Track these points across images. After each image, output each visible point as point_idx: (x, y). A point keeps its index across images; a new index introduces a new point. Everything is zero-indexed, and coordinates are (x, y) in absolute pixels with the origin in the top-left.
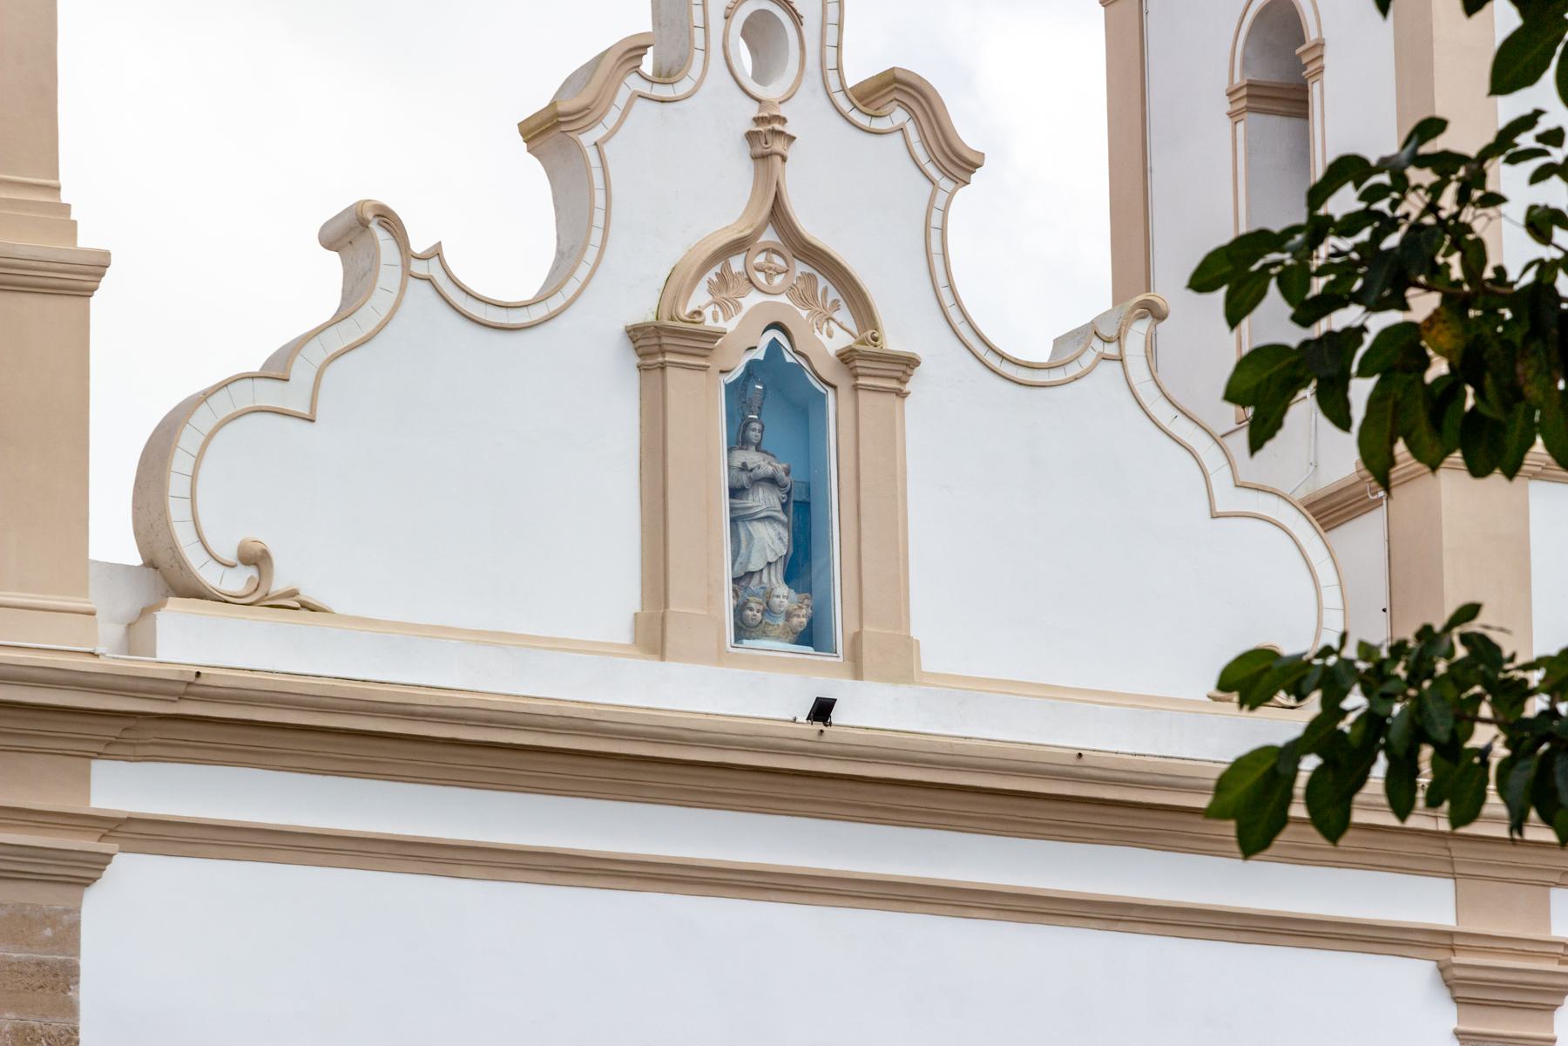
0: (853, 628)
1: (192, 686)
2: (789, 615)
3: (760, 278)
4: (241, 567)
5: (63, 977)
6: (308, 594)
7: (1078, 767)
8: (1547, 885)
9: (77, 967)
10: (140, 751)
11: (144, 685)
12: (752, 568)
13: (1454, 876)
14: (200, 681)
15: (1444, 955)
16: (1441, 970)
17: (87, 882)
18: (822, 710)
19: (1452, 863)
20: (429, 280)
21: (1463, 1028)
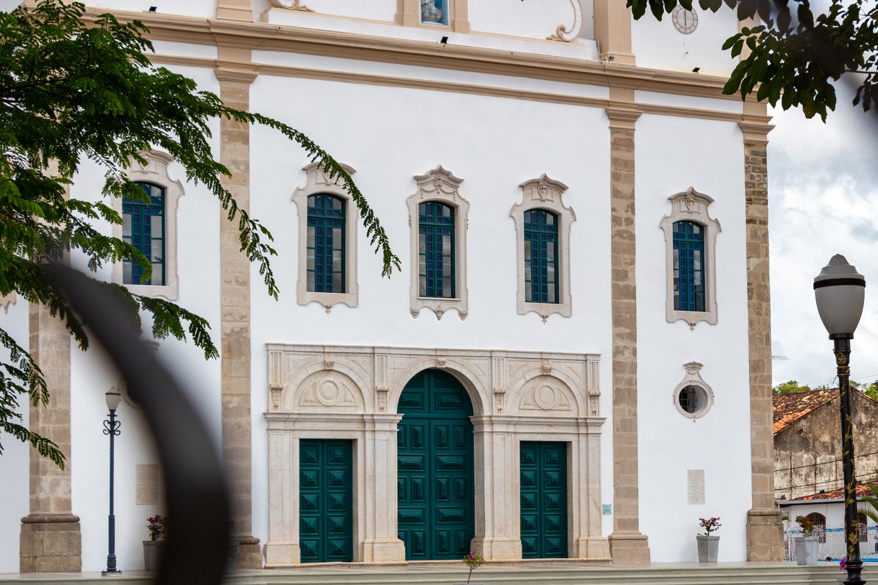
0: (453, 19)
1: (278, 31)
2: (436, 15)
6: (309, 7)
7: (511, 56)
8: (634, 89)
9: (248, 105)
10: (264, 48)
11: (266, 30)
13: (609, 86)
15: (607, 107)
16: (606, 111)
17: (251, 82)
18: (444, 40)
19: (609, 83)
21: (611, 126)
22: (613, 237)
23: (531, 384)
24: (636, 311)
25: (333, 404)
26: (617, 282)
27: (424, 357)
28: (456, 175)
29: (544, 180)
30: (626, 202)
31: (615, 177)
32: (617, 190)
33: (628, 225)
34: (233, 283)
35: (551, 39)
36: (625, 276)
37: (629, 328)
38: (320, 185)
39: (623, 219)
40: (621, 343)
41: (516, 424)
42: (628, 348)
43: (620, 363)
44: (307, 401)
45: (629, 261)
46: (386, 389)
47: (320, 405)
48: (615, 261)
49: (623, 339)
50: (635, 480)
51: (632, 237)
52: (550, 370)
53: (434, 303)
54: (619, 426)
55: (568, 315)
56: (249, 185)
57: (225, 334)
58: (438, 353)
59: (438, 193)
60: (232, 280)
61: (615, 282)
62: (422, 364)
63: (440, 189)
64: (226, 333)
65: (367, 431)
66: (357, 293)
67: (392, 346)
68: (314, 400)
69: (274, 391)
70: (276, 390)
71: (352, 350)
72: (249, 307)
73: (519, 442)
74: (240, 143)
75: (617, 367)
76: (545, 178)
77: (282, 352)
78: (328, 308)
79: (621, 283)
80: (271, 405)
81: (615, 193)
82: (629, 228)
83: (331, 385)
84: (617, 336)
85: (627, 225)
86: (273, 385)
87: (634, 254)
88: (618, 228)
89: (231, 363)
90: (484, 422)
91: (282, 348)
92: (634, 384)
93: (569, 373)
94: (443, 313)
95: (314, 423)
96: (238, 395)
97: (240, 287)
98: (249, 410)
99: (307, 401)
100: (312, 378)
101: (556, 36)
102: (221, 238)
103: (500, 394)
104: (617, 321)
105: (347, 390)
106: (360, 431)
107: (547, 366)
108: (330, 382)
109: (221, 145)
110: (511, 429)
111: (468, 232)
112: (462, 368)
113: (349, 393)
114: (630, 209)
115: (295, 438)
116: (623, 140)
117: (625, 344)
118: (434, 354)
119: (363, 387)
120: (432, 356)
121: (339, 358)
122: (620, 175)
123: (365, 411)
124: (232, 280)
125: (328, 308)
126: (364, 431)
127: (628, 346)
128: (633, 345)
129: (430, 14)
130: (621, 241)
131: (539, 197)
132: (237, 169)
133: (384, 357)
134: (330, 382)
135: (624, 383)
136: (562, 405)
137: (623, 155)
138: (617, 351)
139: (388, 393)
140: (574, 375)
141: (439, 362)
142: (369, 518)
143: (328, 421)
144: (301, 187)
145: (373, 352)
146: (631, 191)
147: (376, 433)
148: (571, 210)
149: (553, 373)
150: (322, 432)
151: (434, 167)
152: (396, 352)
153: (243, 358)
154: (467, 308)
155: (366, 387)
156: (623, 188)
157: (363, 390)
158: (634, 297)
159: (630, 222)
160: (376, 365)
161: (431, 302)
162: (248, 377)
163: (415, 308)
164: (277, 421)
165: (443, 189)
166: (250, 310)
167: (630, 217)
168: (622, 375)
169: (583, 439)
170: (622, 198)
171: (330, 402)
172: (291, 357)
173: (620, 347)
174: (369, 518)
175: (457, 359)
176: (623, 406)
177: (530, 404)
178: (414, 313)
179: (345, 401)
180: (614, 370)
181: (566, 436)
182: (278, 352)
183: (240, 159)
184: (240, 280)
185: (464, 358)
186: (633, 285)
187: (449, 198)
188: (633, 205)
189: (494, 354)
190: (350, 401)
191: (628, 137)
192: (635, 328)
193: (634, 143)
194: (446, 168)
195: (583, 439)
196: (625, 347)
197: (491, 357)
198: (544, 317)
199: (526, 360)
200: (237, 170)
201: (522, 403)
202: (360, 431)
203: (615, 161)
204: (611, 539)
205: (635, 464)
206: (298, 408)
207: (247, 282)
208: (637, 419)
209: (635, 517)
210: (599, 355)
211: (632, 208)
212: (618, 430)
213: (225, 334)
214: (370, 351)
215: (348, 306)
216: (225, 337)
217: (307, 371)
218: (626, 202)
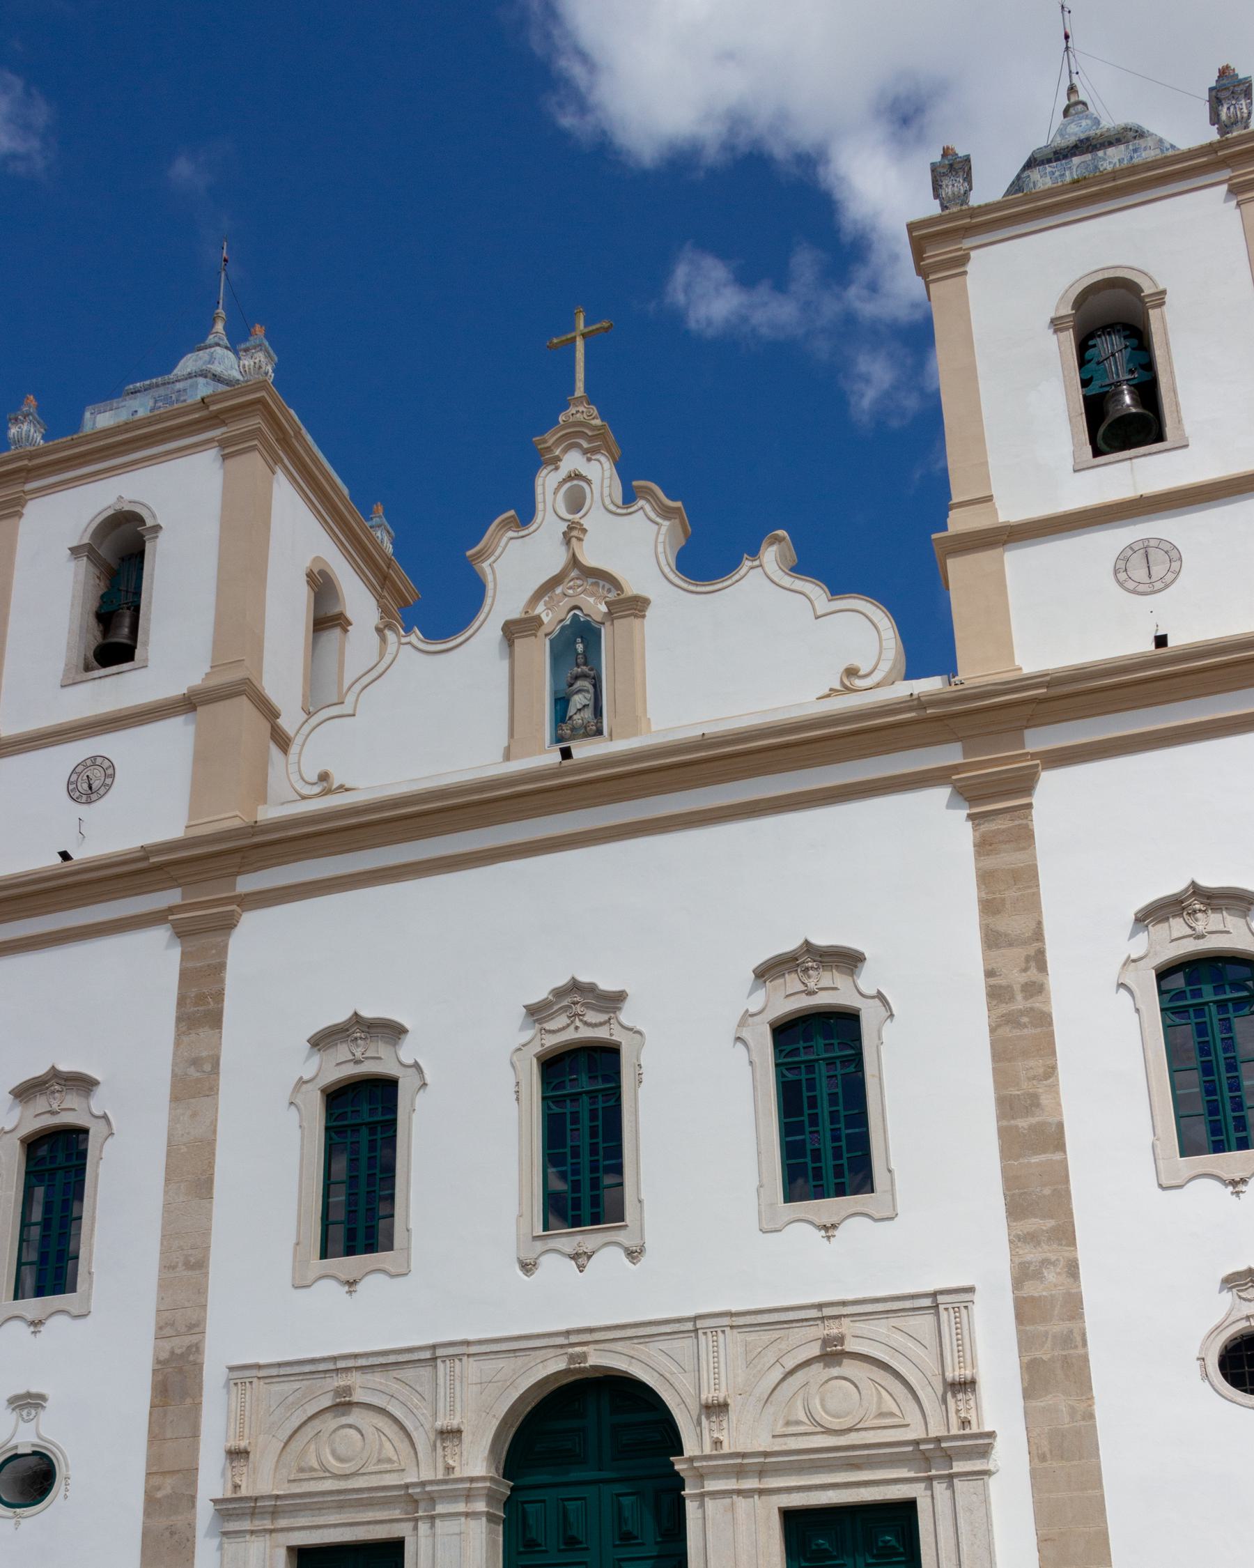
3: (571, 592)
4: (319, 783)
5: (221, 967)
12: (571, 714)
14: (258, 824)
20: (409, 643)
22: (993, 1030)
23: (800, 1376)
24: (1067, 1176)
25: (353, 1470)
26: (1012, 1122)
27: (543, 1351)
28: (606, 984)
29: (808, 951)
30: (1019, 953)
31: (989, 907)
32: (997, 932)
33: (1032, 996)
34: (180, 1267)
35: (828, 696)
36: (1031, 1105)
37: (1052, 1218)
38: (343, 1067)
39: (1017, 988)
40: (1032, 1255)
42: (1054, 1264)
43: (1033, 1299)
44: (301, 1470)
45: (1041, 1070)
46: (455, 1423)
47: (327, 1474)
48: (1002, 1078)
49: (1039, 1243)
51: (1044, 1020)
52: (841, 1339)
53: (570, 1240)
56: (217, 1093)
58: (573, 1339)
59: (577, 1028)
60: (177, 1263)
61: (1005, 1123)
63: (581, 1020)
64: (161, 1358)
67: (471, 1337)
68: (316, 1466)
69: (234, 1456)
70: (237, 1455)
71: (392, 1359)
72: (204, 1307)
73: (776, 1511)
74: (206, 1029)
75: (1026, 1311)
76: (808, 947)
77: (255, 1380)
78: (351, 1283)
79: (1023, 1123)
80: (229, 1486)
81: (992, 940)
82: (1036, 1003)
83: (352, 1432)
85: (1026, 998)
86: (233, 1444)
87: (1054, 1053)
88: (1004, 1009)
90: (682, 1474)
91: (255, 1373)
93: (899, 1339)
94: (589, 1257)
97: (190, 1273)
98: (192, 1499)
99: (301, 1470)
100: (316, 1422)
101: (838, 687)
102: (166, 1193)
103: (716, 1409)
104: (1017, 1207)
105: (384, 1438)
107: (833, 1329)
108: (350, 1426)
109: (175, 1038)
111: (642, 1091)
113: (388, 1443)
114: (1033, 964)
115: (278, 1546)
116: (1004, 831)
118: (566, 1342)
120: (562, 1346)
121: (369, 1376)
122: (1003, 900)
123: (419, 1478)
124: (177, 1263)
125: (351, 1283)
126: (416, 1520)
127: (1053, 1258)
128: (1067, 1254)
129: (573, 729)
130: (1017, 1032)
131: (803, 988)
132: (198, 1071)
133: (457, 1361)
134: (350, 1426)
135: (1049, 1344)
136: (881, 1415)
137: (1007, 859)
138: (1022, 1275)
139: (464, 1434)
140: (911, 1344)
141: (572, 1358)
143: (341, 1506)
144: (306, 1078)
145: (432, 1356)
146: (1033, 925)
147: (438, 1522)
148: (880, 996)
149: (851, 1346)
150: (332, 1530)
151: (562, 981)
152: (484, 1348)
153: (189, 1401)
154: (642, 1237)
155: (421, 1429)
156: (1015, 924)
157: (414, 1435)
158: (1060, 1146)
159: (1036, 989)
160: (441, 1381)
161: (564, 1240)
162: (195, 1434)
163: (529, 1256)
164: (238, 1515)
165: (585, 1019)
166: (205, 1311)
167: (1033, 979)
169: (939, 1487)
170: (1011, 945)
171: (347, 1468)
172: (276, 1388)
173: (1030, 1263)
175: (618, 1346)
177: (798, 1423)
178: (527, 1267)
179: (379, 1461)
180: (1020, 1318)
182: (247, 1380)
183: (204, 1054)
184: (192, 1260)
185: (636, 1341)
186: (1055, 1120)
187: (602, 1034)
188: (1041, 953)
189: (700, 1324)
190: (390, 1461)
191: (1017, 823)
193: (1032, 831)
194: (584, 978)
195: (939, 1487)
196: (1045, 1262)
197: (696, 1330)
198: (828, 1229)
199: (786, 1326)
200: (199, 1074)
201: (781, 1422)
203: (985, 878)
206: (286, 1485)
207: (204, 1262)
210: (971, 1290)
211: (1039, 961)
214: (427, 1355)
215: (393, 1276)
216: (159, 1367)
217: (305, 1411)
218: (1019, 953)
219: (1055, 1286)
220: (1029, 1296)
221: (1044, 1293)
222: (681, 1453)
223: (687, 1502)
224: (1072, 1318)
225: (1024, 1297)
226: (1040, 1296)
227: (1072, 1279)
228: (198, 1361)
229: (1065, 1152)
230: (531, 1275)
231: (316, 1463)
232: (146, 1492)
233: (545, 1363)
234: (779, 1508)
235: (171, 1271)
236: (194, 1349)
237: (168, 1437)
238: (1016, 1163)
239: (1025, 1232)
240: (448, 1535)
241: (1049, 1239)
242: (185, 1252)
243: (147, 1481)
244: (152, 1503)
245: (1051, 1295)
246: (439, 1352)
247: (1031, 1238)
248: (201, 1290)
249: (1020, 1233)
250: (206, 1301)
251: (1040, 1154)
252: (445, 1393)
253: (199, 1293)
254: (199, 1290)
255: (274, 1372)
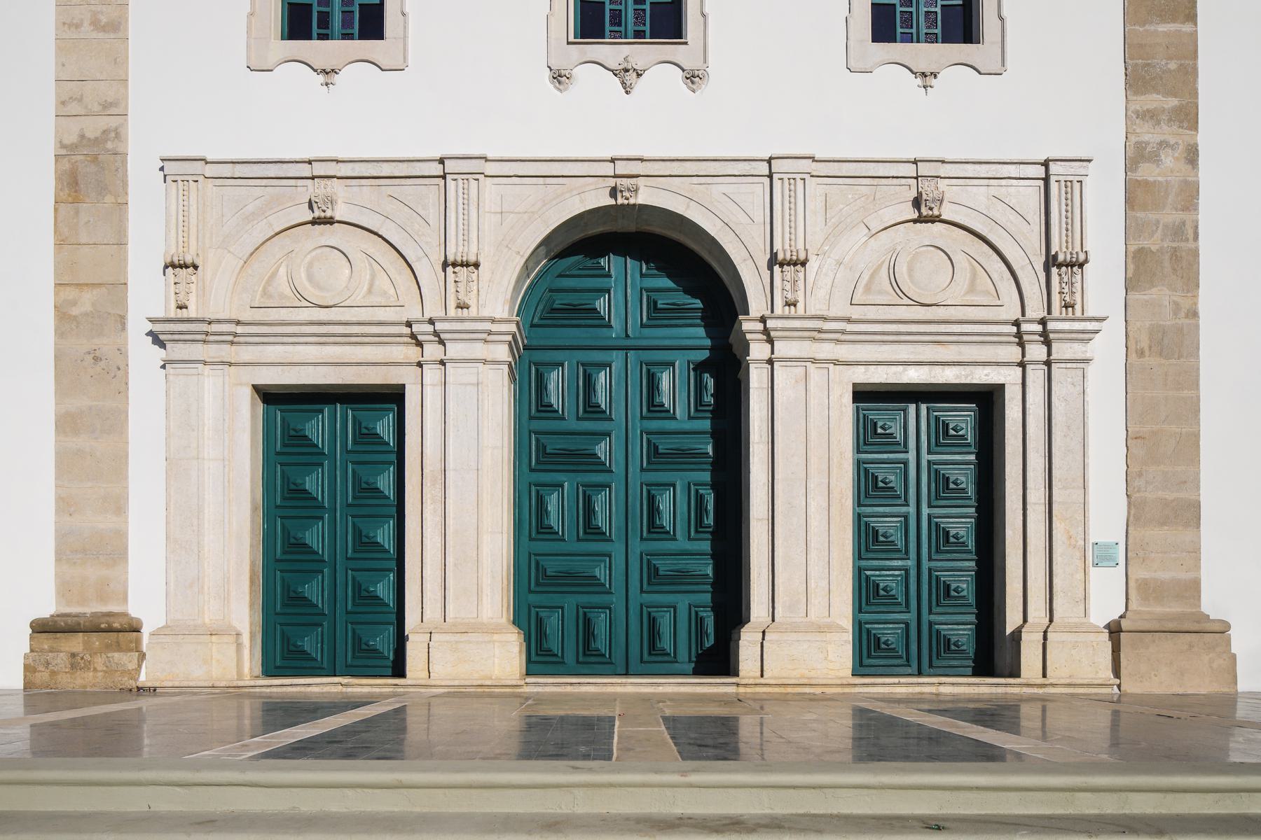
24: (1196, 51)
34: (86, 26)
40: (1149, 135)
41: (840, 338)
42: (1173, 147)
43: (1147, 183)
49: (1158, 123)
50: (1195, 482)
54: (1145, 344)
55: (997, 69)
57: (63, 146)
62: (577, 199)
64: (66, 142)
65: (428, 362)
66: (405, 37)
71: (386, 170)
77: (201, 179)
80: (173, 305)
84: (1136, 117)
89: (77, 213)
90: (748, 336)
92: (1191, 236)
93: (999, 212)
94: (639, 75)
95: (290, 348)
96: (94, 285)
97: (101, 35)
98: (122, 321)
106: (410, 364)
110: (826, 350)
112: (688, 206)
115: (241, 384)
117: (1162, 138)
119: (419, 259)
124: (82, 20)
135: (1159, 234)
138: (1137, 156)
142: (433, 573)
143: (324, 339)
153: (109, 199)
158: (1192, 17)
162: (122, 244)
166: (126, 87)
168: (1152, 216)
173: (1147, 143)
174: (433, 573)
176: (1160, 294)
180: (1130, 202)
181: (988, 370)
184: (104, 20)
192: (1195, 94)
196: (1163, 144)
202: (410, 364)
204: (1114, 630)
205: (1194, 440)
208: (1197, 326)
209: (1191, 575)
212: (1141, 353)
213: (63, 146)
214: (436, 169)
217: (271, 225)
219: (1172, 172)
220: (1143, 180)
221: (1160, 179)
222: (747, 313)
223: (752, 367)
224: (1186, 209)
225: (1137, 180)
226: (1155, 181)
227: (1191, 166)
228: (120, 150)
229: (1196, 24)
230: (566, 89)
231: (289, 289)
232: (55, 307)
233: (582, 195)
234: (854, 385)
235: (73, 29)
236: (113, 135)
237: (83, 241)
238: (1141, 29)
239: (1145, 109)
240: (459, 384)
241: (1170, 120)
242: (93, 8)
243: (56, 294)
244: (64, 317)
245: (1166, 181)
246: (450, 166)
247: (1150, 116)
248: (119, 60)
249: (1139, 108)
250: (127, 75)
251: (1169, 23)
252: (457, 218)
253: (115, 63)
254: (115, 60)
255: (226, 170)
